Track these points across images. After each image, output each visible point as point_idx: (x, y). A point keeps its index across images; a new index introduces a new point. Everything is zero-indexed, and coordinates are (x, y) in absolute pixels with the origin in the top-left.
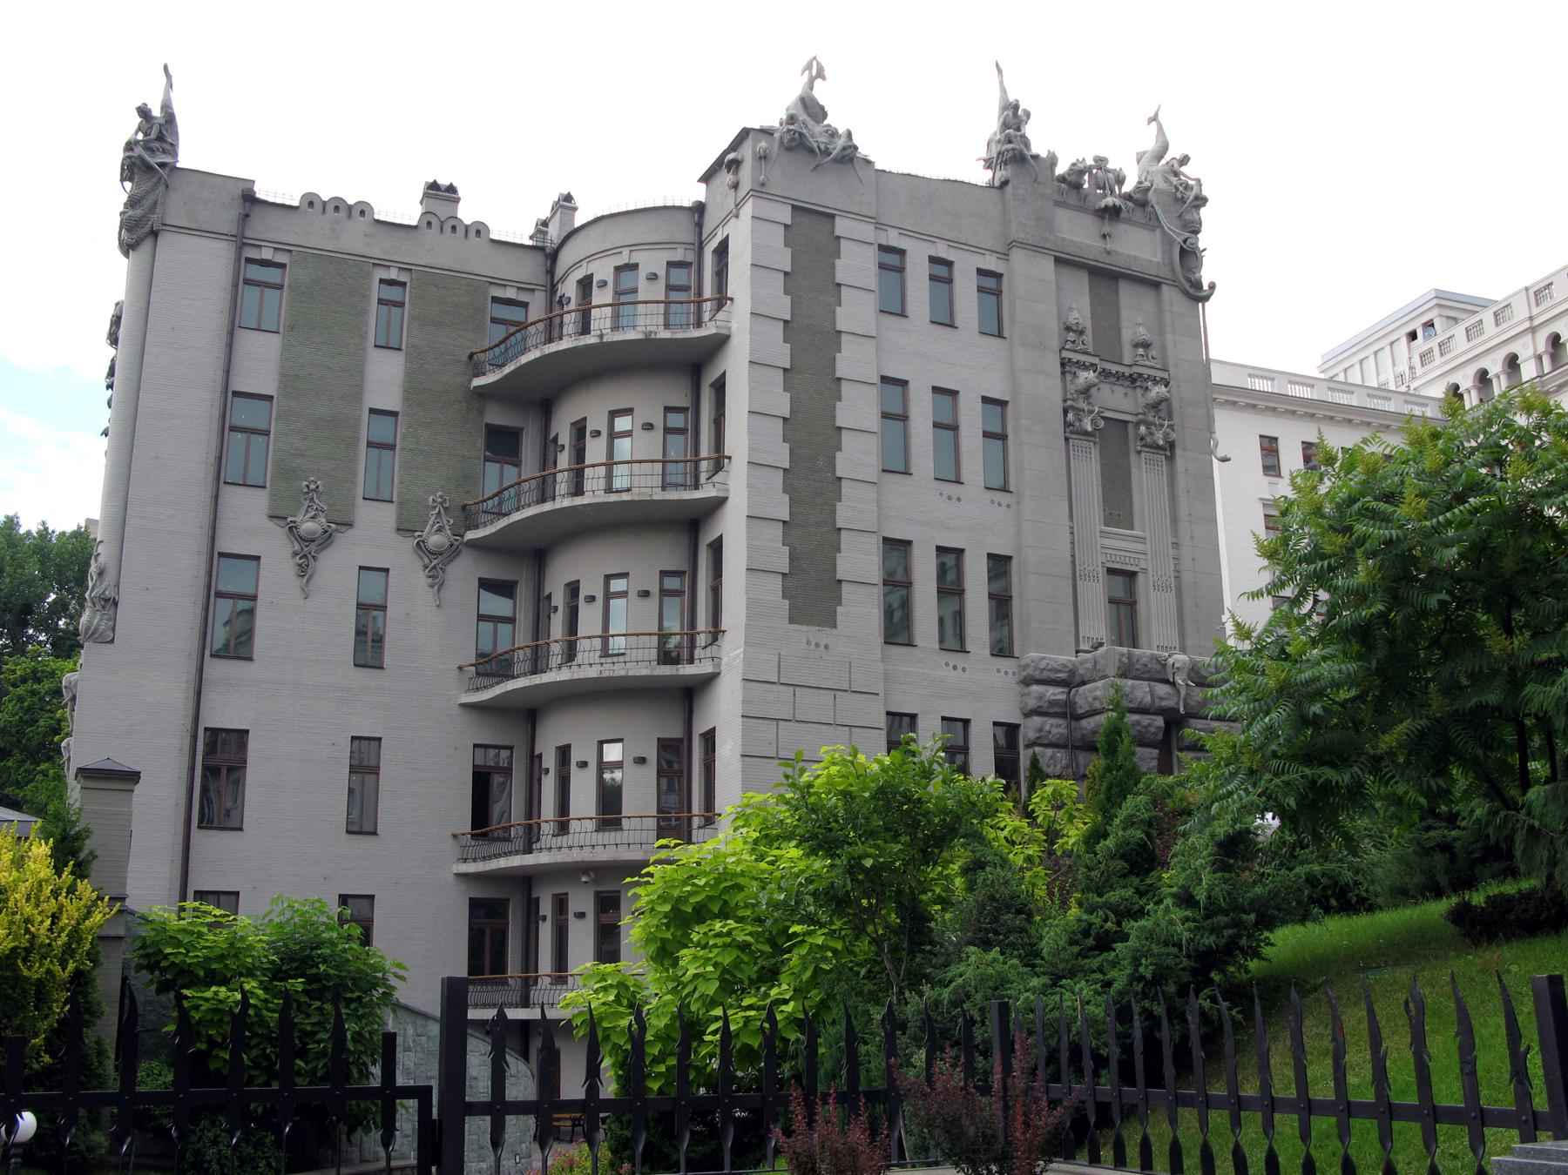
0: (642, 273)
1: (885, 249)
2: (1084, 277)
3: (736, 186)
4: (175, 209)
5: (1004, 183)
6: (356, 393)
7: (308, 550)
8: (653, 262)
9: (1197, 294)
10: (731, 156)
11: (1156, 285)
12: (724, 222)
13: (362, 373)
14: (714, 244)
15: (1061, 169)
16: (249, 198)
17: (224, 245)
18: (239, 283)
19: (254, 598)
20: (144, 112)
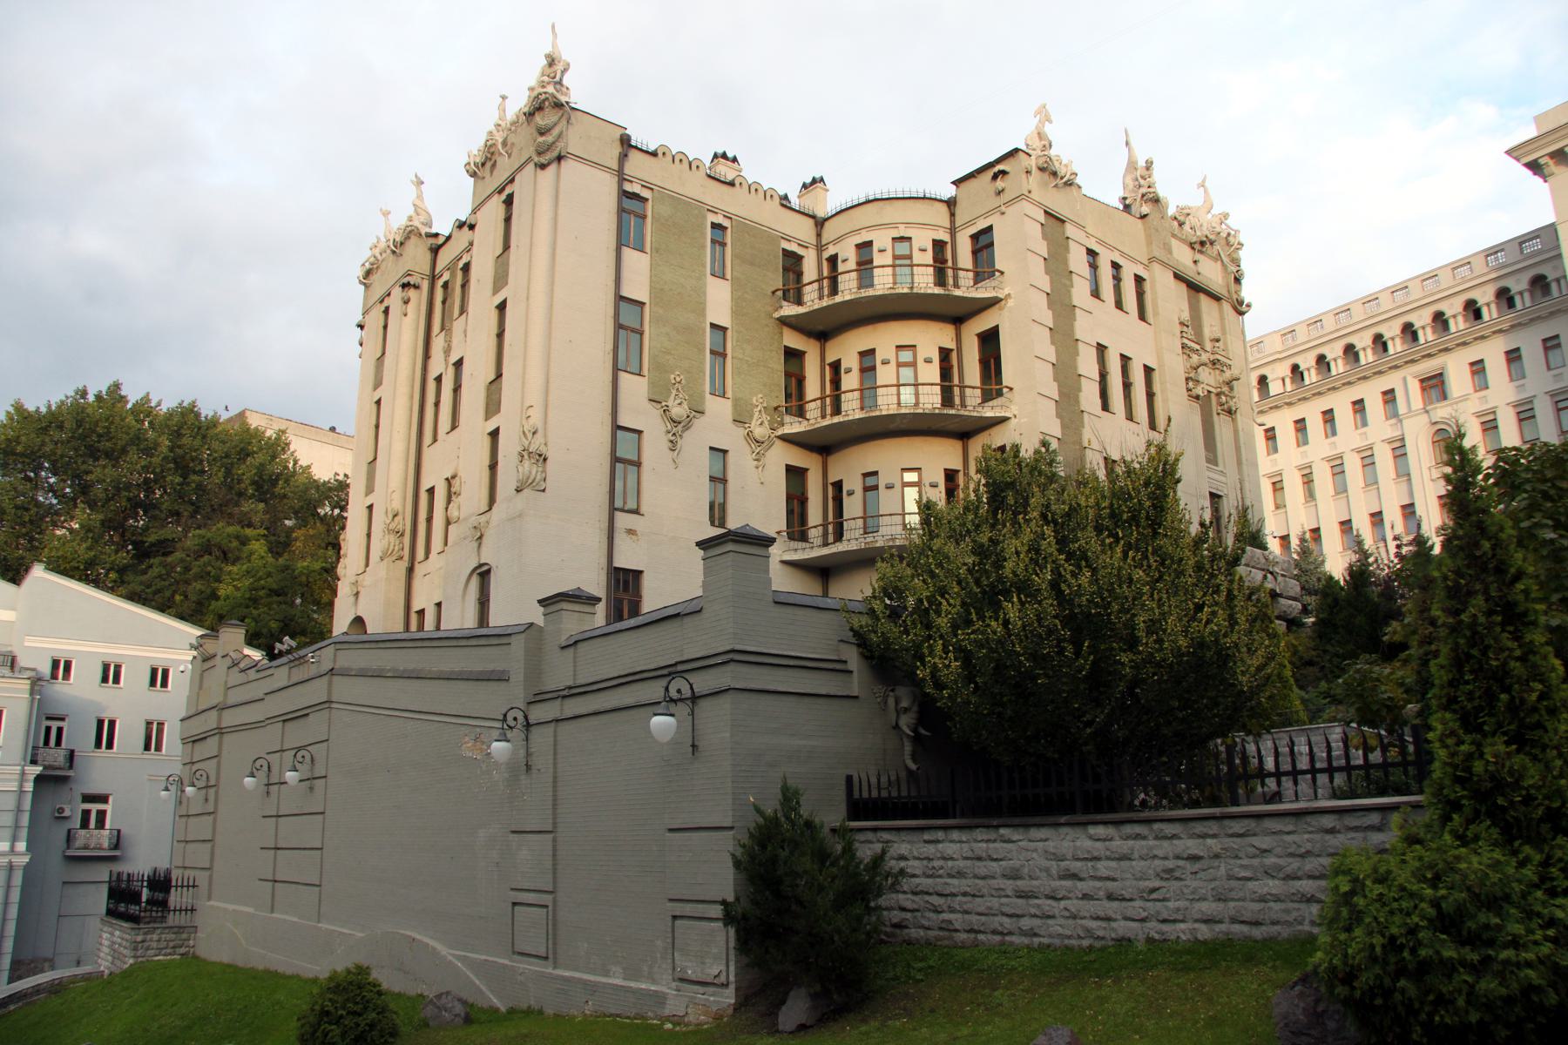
0: (916, 245)
1: (1091, 253)
2: (1183, 287)
3: (999, 193)
4: (573, 142)
5: (1143, 217)
6: (701, 310)
7: (678, 427)
8: (923, 239)
9: (1240, 308)
10: (1000, 167)
11: (1217, 298)
12: (987, 214)
13: (705, 293)
14: (974, 230)
15: (1171, 211)
16: (625, 141)
17: (607, 176)
18: (621, 211)
19: (638, 464)
20: (547, 56)
